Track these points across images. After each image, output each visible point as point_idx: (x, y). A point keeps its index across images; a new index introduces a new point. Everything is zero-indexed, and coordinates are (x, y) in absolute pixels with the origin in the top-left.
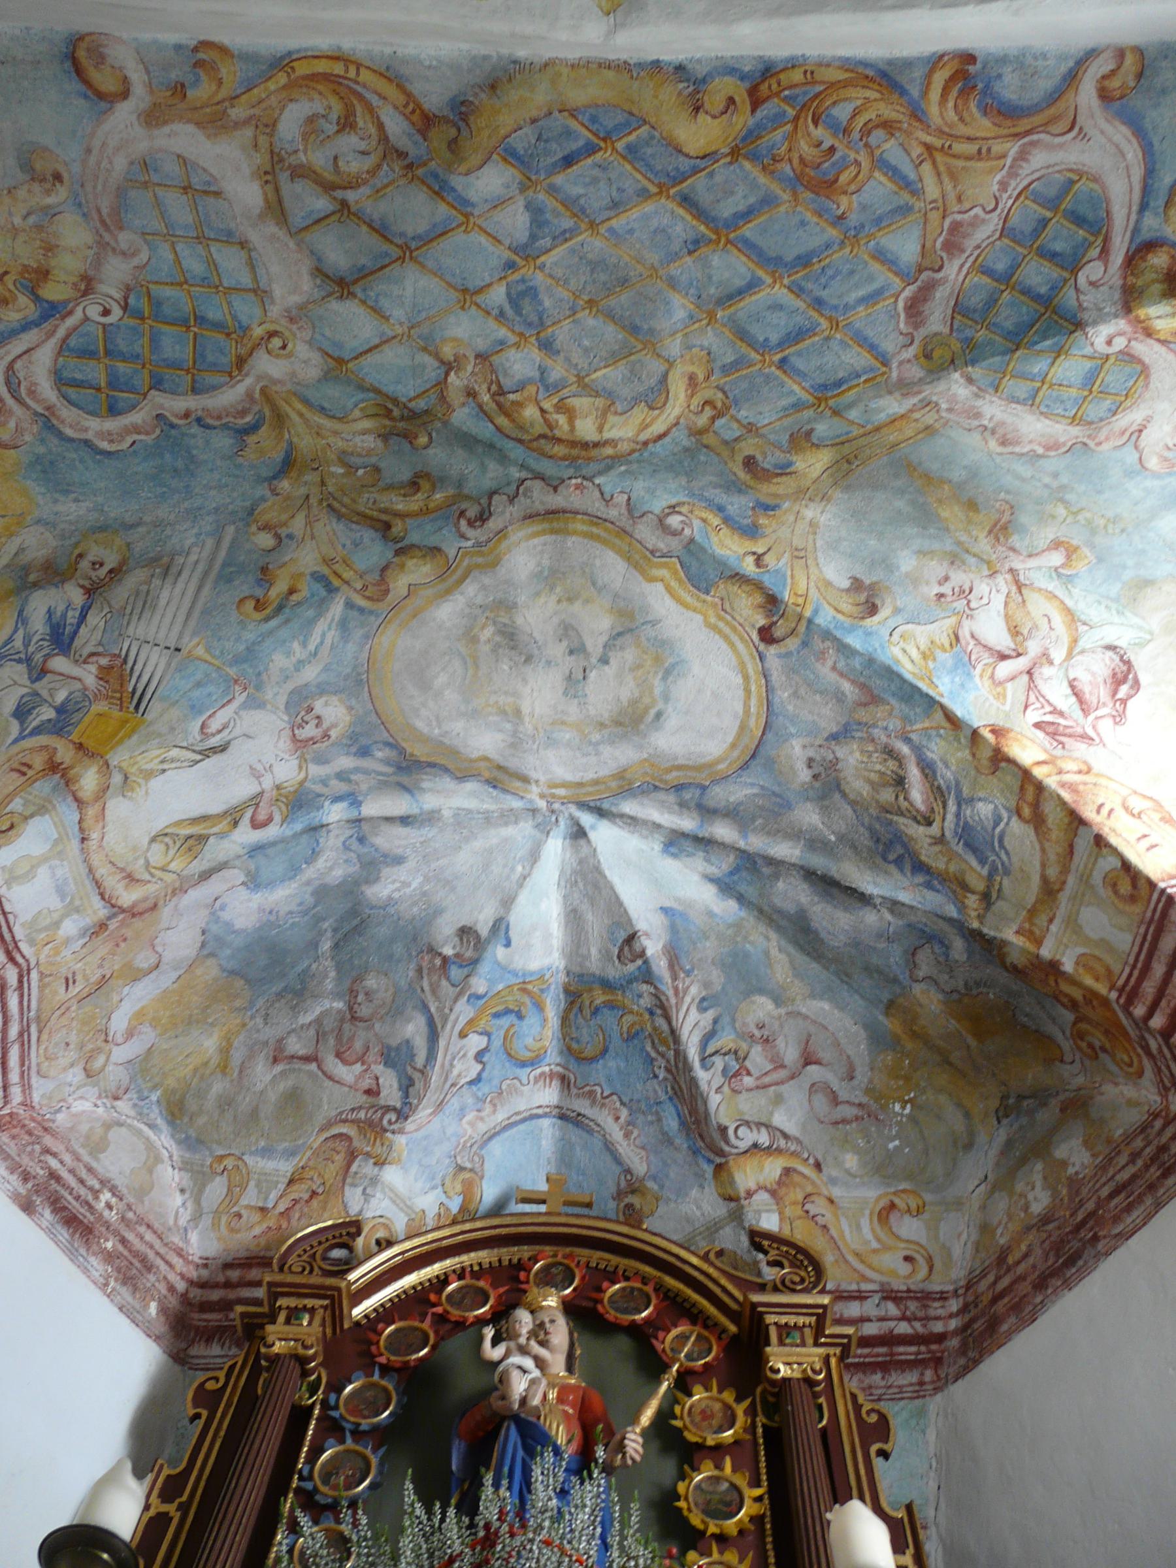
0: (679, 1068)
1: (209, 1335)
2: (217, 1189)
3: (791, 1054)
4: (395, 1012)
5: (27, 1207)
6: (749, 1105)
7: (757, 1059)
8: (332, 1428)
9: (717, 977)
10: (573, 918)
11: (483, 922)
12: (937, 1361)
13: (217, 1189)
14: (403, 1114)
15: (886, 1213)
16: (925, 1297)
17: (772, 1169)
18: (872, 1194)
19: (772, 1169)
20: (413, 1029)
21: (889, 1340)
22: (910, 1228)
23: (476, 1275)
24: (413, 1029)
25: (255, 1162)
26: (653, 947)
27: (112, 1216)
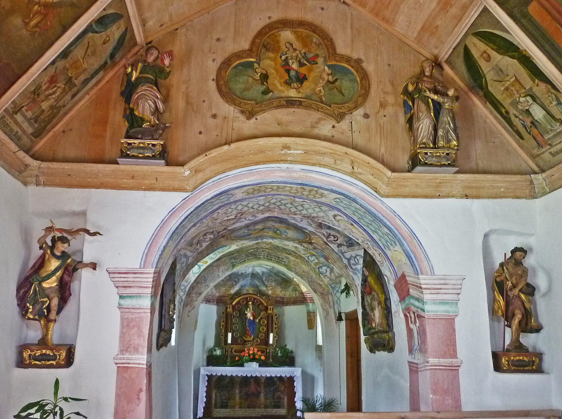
0: (263, 281)
1: (220, 303)
2: (218, 290)
3: (274, 280)
4: (235, 278)
5: (206, 303)
6: (269, 283)
7: (270, 281)
8: (234, 317)
9: (267, 276)
10: (252, 270)
11: (244, 272)
12: (284, 304)
13: (218, 290)
14: (236, 285)
15: (281, 291)
16: (284, 298)
17: (271, 288)
18: (280, 290)
19: (271, 288)
20: (237, 279)
21: (280, 301)
22: (283, 292)
23: (244, 298)
24: (237, 279)
25: (222, 288)
26: (261, 274)
27: (211, 298)
